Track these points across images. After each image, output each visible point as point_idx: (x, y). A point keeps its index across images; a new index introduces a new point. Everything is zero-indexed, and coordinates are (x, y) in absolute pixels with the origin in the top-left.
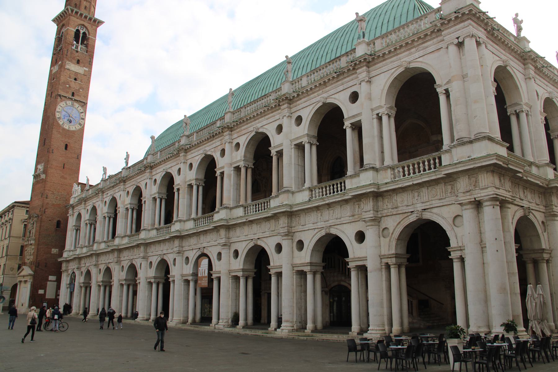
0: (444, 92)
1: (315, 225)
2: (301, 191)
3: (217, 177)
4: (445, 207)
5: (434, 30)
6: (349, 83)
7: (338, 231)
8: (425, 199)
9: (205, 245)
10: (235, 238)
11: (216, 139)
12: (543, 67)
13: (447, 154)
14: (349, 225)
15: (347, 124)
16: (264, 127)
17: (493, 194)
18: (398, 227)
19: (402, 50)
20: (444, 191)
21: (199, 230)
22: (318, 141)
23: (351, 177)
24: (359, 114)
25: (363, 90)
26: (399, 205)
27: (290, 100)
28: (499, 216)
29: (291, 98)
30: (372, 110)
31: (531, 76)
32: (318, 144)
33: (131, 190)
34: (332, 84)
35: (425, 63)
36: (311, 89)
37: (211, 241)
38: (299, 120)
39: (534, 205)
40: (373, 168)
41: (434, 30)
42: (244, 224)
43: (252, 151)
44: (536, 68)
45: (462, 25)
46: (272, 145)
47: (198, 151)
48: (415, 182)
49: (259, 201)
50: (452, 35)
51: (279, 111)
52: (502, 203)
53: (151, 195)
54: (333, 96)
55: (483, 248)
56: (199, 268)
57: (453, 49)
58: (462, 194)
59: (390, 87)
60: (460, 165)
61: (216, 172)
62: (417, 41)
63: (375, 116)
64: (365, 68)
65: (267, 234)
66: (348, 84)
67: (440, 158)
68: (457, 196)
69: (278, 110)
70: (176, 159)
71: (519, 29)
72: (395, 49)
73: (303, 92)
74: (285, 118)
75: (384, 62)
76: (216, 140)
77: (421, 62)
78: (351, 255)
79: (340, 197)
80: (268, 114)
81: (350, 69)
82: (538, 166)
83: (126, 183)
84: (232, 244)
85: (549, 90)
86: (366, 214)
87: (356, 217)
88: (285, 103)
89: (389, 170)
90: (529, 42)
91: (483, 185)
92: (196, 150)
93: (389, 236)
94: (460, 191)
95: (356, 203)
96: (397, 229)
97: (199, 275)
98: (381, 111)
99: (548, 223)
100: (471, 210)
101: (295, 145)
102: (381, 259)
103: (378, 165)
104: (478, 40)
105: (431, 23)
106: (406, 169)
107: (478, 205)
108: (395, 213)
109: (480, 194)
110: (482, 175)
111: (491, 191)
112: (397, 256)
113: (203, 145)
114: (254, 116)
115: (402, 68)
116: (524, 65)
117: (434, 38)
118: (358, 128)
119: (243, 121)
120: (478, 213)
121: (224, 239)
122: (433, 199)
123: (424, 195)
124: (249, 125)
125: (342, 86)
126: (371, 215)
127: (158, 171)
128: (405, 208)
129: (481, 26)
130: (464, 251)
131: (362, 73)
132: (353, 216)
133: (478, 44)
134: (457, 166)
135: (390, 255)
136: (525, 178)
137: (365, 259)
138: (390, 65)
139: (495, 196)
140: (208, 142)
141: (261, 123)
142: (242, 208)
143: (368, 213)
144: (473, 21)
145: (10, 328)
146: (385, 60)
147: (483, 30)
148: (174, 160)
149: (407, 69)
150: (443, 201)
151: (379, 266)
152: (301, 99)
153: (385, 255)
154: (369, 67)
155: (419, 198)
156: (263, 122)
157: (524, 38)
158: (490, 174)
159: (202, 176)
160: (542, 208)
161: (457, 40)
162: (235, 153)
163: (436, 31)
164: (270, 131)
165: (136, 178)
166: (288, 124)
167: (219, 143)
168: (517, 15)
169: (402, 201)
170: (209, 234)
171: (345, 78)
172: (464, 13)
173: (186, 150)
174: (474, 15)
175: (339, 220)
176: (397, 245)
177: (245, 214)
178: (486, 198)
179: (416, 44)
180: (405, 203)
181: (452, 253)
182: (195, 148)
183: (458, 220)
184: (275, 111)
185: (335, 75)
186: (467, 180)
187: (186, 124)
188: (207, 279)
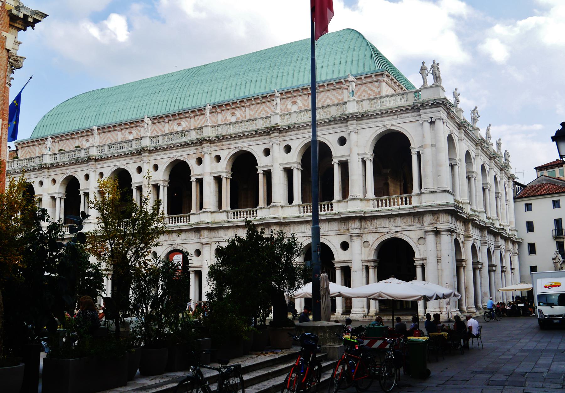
0: (417, 153)
1: (304, 234)
2: (290, 206)
3: (192, 182)
4: (413, 231)
5: (414, 107)
6: (338, 129)
7: (325, 240)
8: (399, 224)
10: (217, 239)
11: (190, 147)
12: (468, 130)
13: (416, 196)
14: (335, 236)
15: (335, 161)
16: (249, 147)
17: (449, 228)
18: (376, 241)
19: (387, 115)
20: (413, 221)
21: (174, 229)
22: (302, 167)
23: (338, 202)
24: (349, 156)
25: (352, 139)
26: (378, 226)
27: (281, 131)
28: (450, 241)
29: (282, 129)
30: (358, 155)
31: (463, 139)
32: (302, 169)
33: (60, 179)
34: (322, 126)
35: (403, 129)
36: (303, 126)
37: (187, 239)
38: (288, 149)
39: (460, 230)
40: (358, 199)
41: (414, 107)
42: (229, 227)
43: (231, 164)
44: (465, 131)
45: (435, 109)
46: (259, 165)
47: (167, 154)
48: (393, 213)
49: (245, 209)
50: (427, 114)
51: (267, 137)
52: (451, 232)
54: (322, 136)
55: (439, 259)
57: (427, 125)
58: (427, 225)
59: (373, 140)
60: (429, 207)
61: (190, 178)
62: (399, 112)
63: (361, 159)
64: (355, 121)
66: (337, 129)
67: (410, 198)
68: (424, 225)
69: (266, 135)
71: (458, 102)
72: (382, 113)
73: (295, 127)
74: (275, 145)
75: (371, 120)
76: (191, 148)
77: (401, 128)
78: (336, 259)
79: (331, 216)
80: (255, 137)
81: (341, 119)
82: (462, 204)
83: (50, 170)
84: (213, 243)
85: (468, 144)
86: (353, 230)
87: (342, 231)
88: (276, 132)
89: (371, 201)
90: (463, 112)
91: (443, 221)
92: (163, 153)
93: (368, 247)
94: (426, 223)
95: (342, 222)
96: (375, 243)
98: (365, 157)
99: (466, 242)
100: (432, 236)
101: (283, 168)
102: (362, 262)
103: (362, 197)
104: (444, 121)
105: (413, 103)
106: (384, 201)
107: (437, 233)
108: (374, 232)
109: (440, 227)
110: (442, 215)
111: (447, 226)
112: (374, 261)
113: (173, 150)
114: (240, 136)
115: (385, 128)
116: (459, 129)
117: (412, 112)
118: (344, 165)
119: (227, 138)
120: (436, 237)
121: (206, 239)
122: (405, 225)
123: (398, 221)
124: (232, 142)
125: (332, 130)
126: (357, 231)
127: (105, 165)
128: (382, 229)
129: (445, 110)
130: (425, 261)
131: (353, 125)
132: (339, 230)
133: (443, 123)
134: (427, 207)
135: (370, 260)
136: (460, 214)
137: (351, 262)
138: (375, 123)
139: (450, 229)
140: (180, 148)
141: (247, 143)
142: (225, 214)
143: (354, 230)
144: (442, 107)
146: (372, 118)
147: (446, 113)
148: (132, 157)
149: (388, 130)
150: (412, 227)
151: (361, 268)
152: (290, 131)
153: (366, 260)
154: (357, 121)
155: (394, 223)
156: (248, 143)
157: (461, 110)
158: (447, 215)
159: (167, 178)
160: (479, 238)
161: (430, 119)
162: (215, 163)
163: (415, 108)
164: (258, 152)
165: (69, 167)
166: (278, 151)
167: (195, 151)
168: (456, 89)
169: (381, 224)
170: (183, 233)
171: (335, 124)
172: (439, 102)
173: (150, 151)
174: (444, 104)
175: (327, 232)
176: (374, 253)
177: (228, 218)
178: (444, 229)
179: (398, 113)
180: (383, 226)
181: (416, 261)
182: (162, 151)
183: (421, 240)
184: (263, 136)
185: (327, 121)
186: (431, 216)
187: (148, 124)
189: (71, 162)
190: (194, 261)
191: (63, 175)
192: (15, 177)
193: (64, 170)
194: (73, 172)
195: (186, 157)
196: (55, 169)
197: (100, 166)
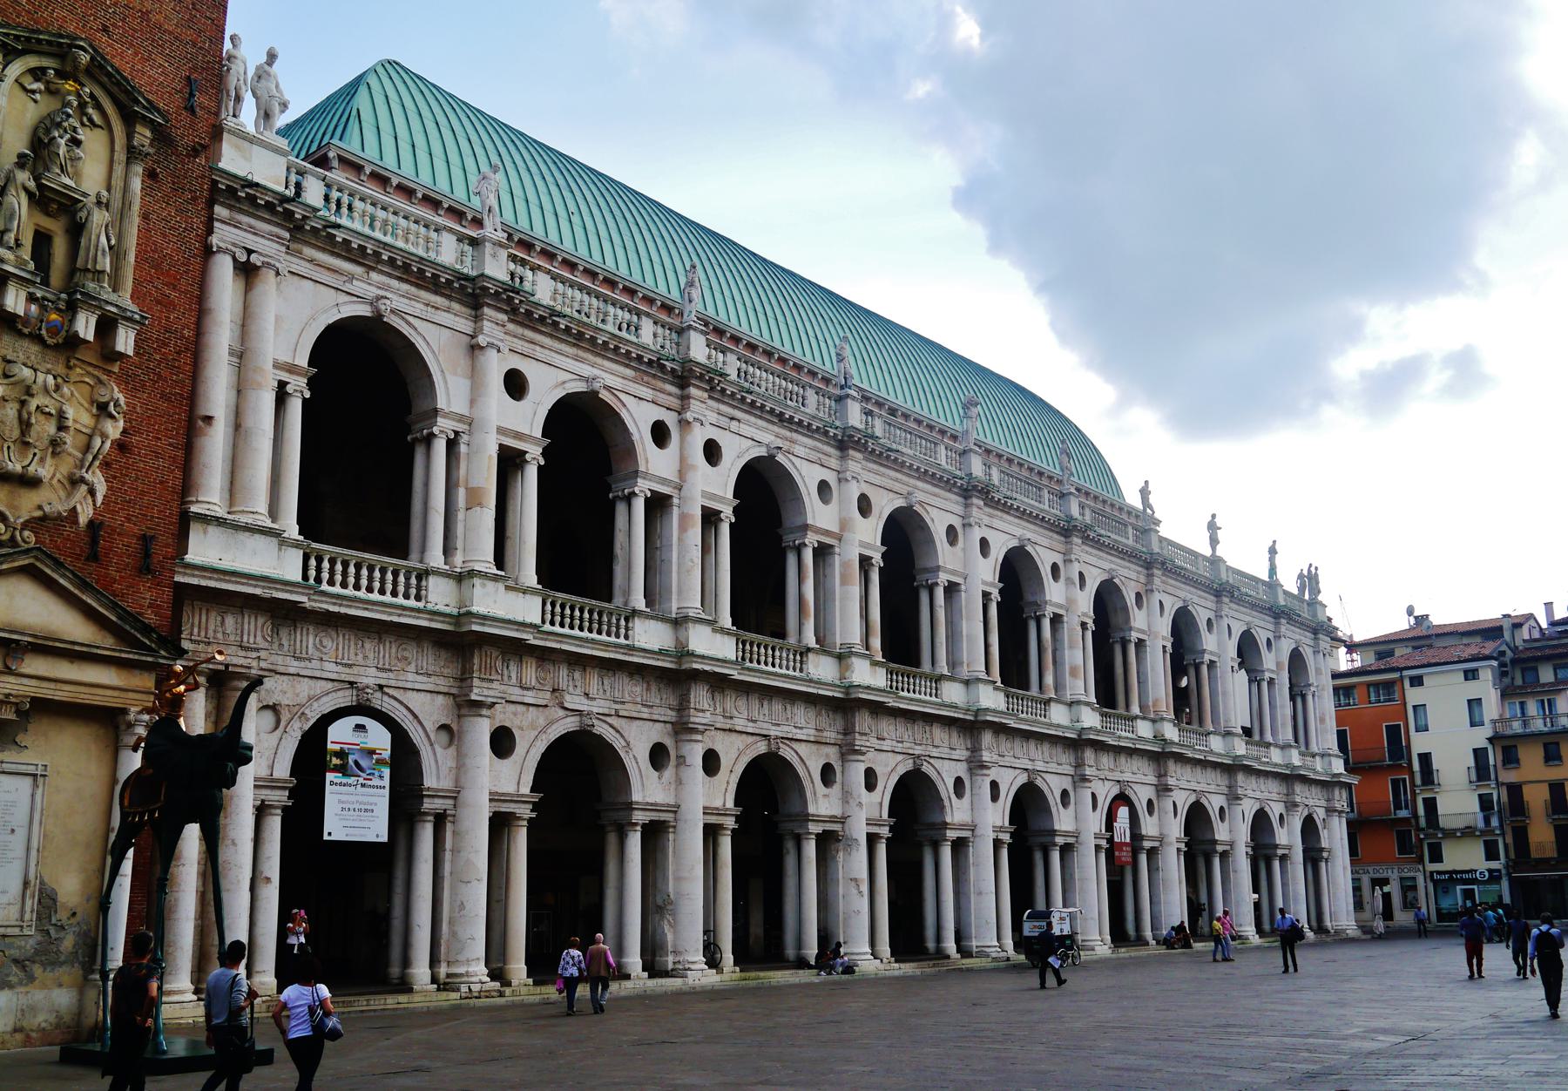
9: (1127, 777)
33: (884, 505)
47: (1100, 558)
51: (1212, 598)
53: (984, 583)
56: (1115, 824)
65: (1212, 788)
70: (1051, 534)
97: (1116, 840)
113: (1108, 553)
127: (997, 523)
131: (1285, 628)
145: (1476, 975)
148: (1047, 532)
167: (1133, 575)
188: (1129, 849)
189: (931, 471)
190: (1149, 826)
191: (891, 495)
192: (732, 419)
193: (897, 480)
194: (920, 503)
195: (1123, 579)
196: (875, 467)
197: (986, 520)
